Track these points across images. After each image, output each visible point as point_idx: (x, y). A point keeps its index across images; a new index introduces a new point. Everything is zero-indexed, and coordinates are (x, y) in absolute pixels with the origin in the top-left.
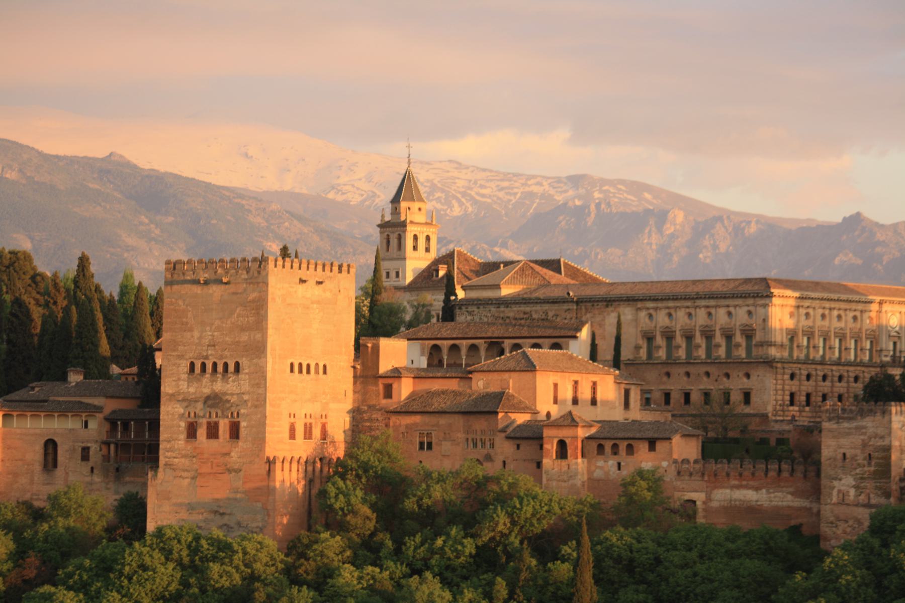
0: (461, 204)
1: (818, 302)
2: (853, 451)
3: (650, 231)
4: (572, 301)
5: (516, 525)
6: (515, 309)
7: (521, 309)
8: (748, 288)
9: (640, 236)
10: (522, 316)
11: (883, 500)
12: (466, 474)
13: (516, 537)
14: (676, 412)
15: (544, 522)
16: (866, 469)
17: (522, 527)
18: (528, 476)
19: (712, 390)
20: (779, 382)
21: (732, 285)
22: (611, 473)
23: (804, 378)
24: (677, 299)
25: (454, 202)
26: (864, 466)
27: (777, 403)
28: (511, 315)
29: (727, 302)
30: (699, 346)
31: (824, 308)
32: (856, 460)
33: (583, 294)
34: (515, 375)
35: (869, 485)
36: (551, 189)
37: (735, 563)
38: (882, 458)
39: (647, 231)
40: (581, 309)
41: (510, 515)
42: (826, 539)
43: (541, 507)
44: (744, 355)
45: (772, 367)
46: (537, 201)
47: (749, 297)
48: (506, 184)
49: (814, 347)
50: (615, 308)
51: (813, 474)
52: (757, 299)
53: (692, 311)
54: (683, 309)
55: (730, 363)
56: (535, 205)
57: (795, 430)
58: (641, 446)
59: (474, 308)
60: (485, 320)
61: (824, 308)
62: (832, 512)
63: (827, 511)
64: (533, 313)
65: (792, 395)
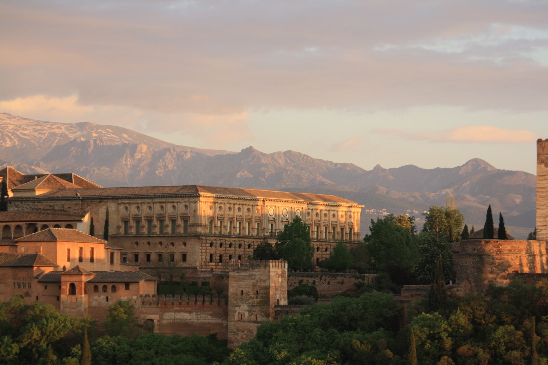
0: (11, 140)
1: (227, 200)
2: (247, 290)
3: (126, 157)
4: (79, 199)
5: (44, 335)
6: (44, 204)
7: (48, 203)
8: (185, 191)
9: (120, 160)
10: (48, 208)
11: (265, 319)
12: (14, 304)
13: (44, 343)
14: (141, 266)
15: (62, 333)
16: (255, 300)
17: (48, 336)
18: (51, 305)
19: (163, 252)
20: (204, 248)
21: (175, 190)
22: (102, 303)
23: (218, 245)
24: (142, 198)
25: (7, 139)
26: (254, 298)
27: (202, 260)
28: (42, 207)
29: (172, 200)
30: (156, 226)
31: (230, 204)
32: (249, 295)
33: (86, 194)
34: (43, 244)
35: (257, 309)
36: (66, 131)
37: (177, 357)
38: (264, 294)
39: (124, 157)
40: (84, 204)
41: (41, 329)
42: (231, 342)
43: (60, 324)
44: (182, 232)
45: (199, 239)
46: (58, 138)
47: (186, 197)
48: (39, 128)
49: (224, 227)
50: (105, 203)
51: (223, 303)
52: (190, 198)
53: (152, 205)
54: (146, 204)
55: (174, 236)
56: (57, 140)
57: (213, 277)
58: (121, 287)
59: (19, 203)
60: (26, 210)
61: (230, 204)
62: (235, 326)
63: (232, 325)
64: (55, 206)
65: (211, 256)
